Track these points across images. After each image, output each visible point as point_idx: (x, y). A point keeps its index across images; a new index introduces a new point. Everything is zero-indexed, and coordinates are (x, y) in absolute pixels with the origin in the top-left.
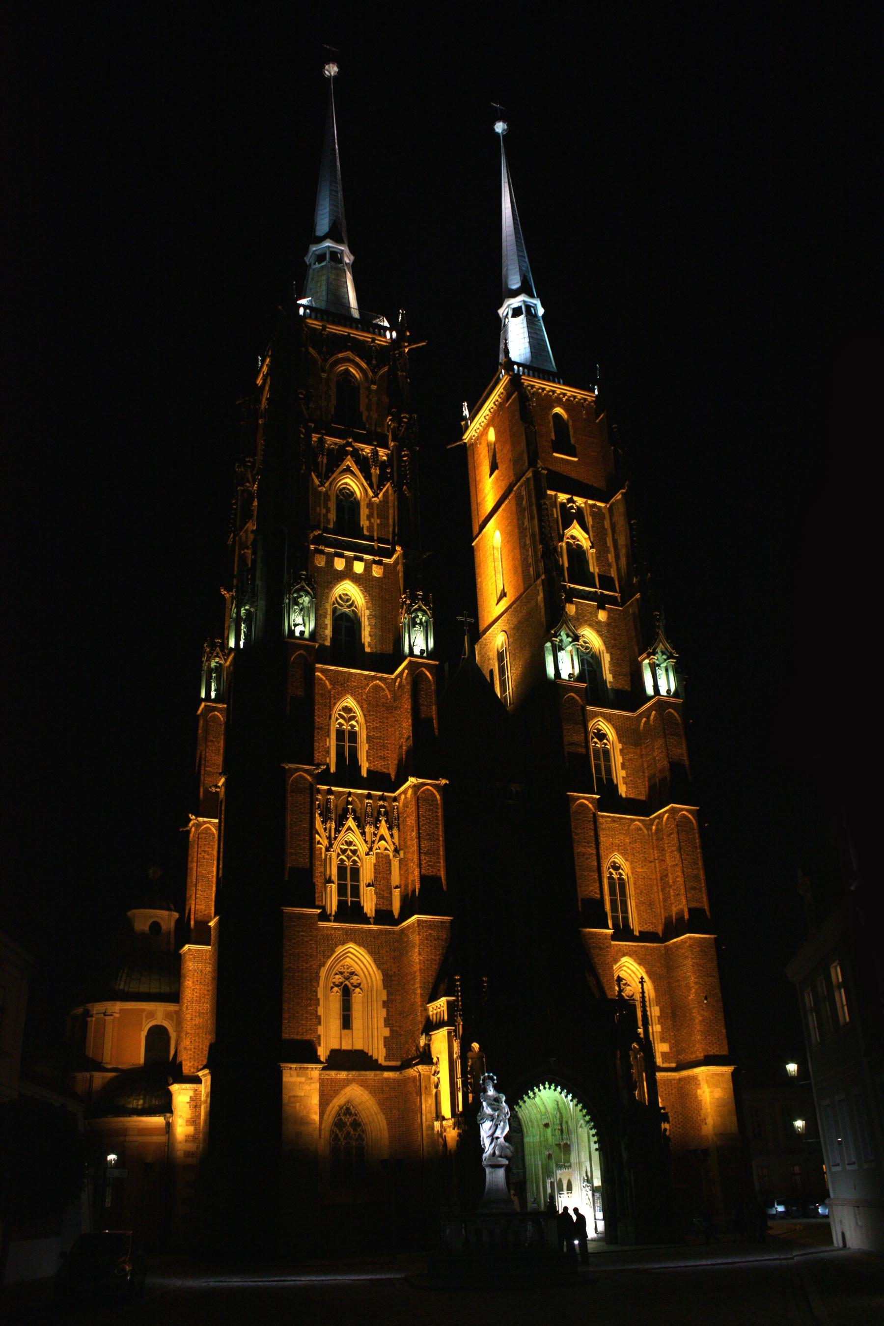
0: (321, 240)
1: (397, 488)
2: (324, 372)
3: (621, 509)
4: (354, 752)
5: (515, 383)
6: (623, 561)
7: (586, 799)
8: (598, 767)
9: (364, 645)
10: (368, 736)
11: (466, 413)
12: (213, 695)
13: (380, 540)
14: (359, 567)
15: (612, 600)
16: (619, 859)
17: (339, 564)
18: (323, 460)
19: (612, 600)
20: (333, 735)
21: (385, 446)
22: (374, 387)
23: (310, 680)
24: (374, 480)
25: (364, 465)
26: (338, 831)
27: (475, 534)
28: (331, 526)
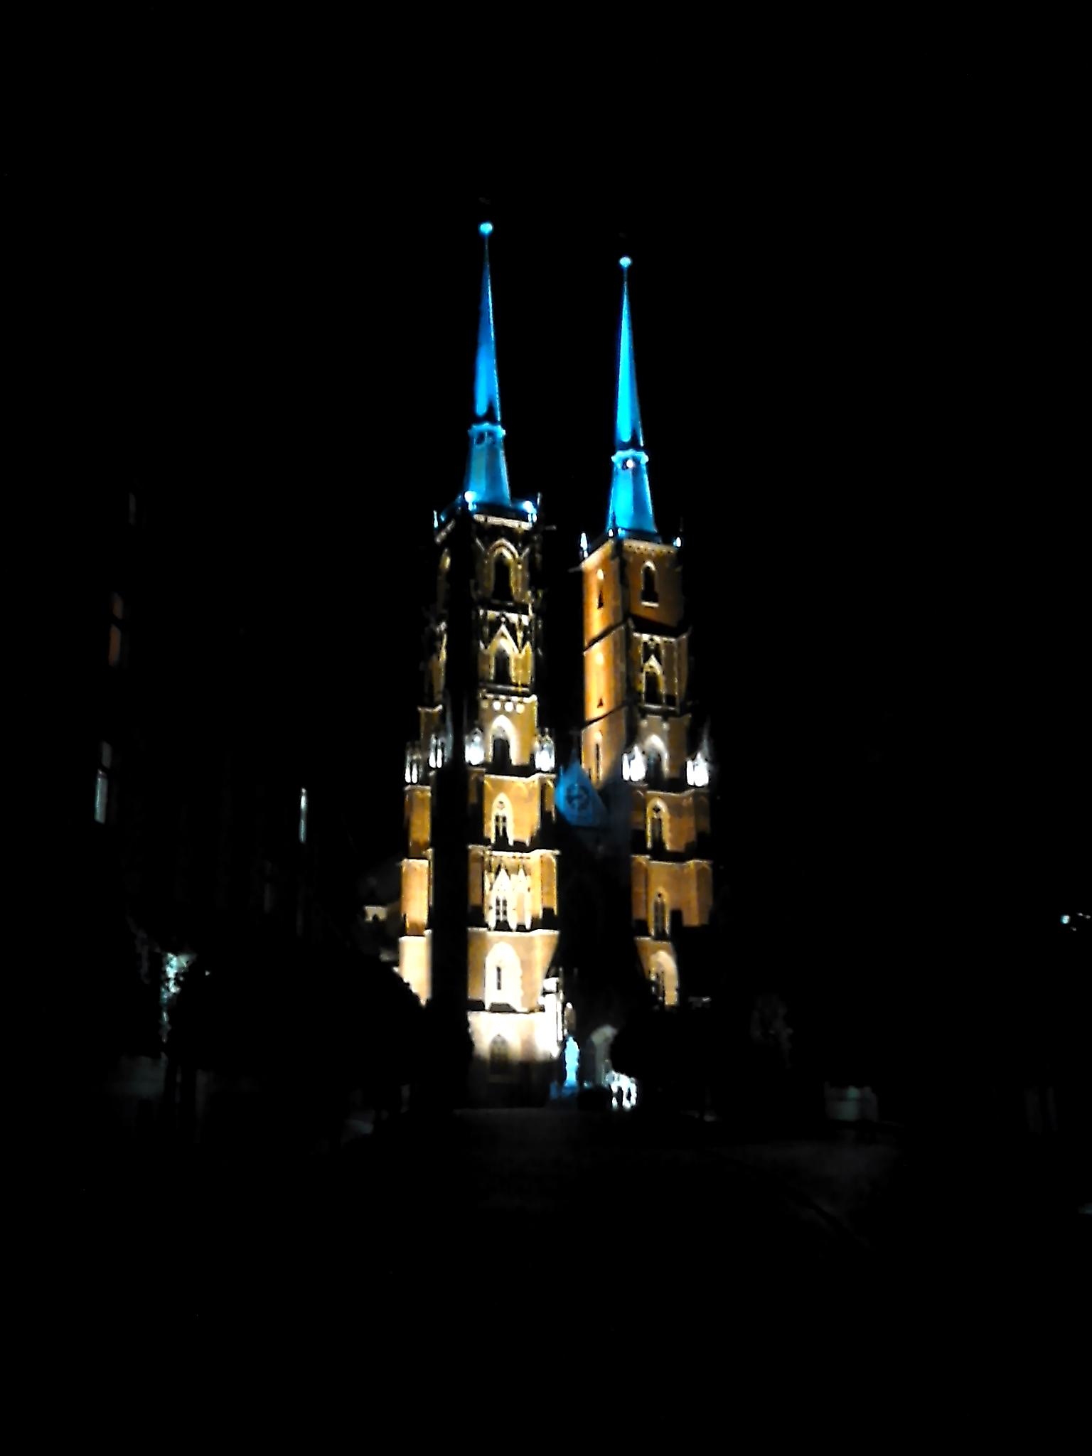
0: (479, 420)
1: (534, 649)
2: (486, 557)
3: (685, 647)
4: (504, 830)
5: (619, 546)
6: (684, 686)
7: (643, 859)
8: (653, 831)
9: (511, 761)
10: (515, 821)
11: (584, 543)
12: (415, 781)
13: (524, 686)
14: (509, 707)
15: (673, 714)
16: (661, 890)
17: (497, 705)
18: (487, 630)
19: (673, 714)
20: (493, 818)
21: (527, 614)
22: (520, 567)
23: (481, 786)
24: (520, 641)
25: (512, 629)
26: (496, 878)
27: (586, 644)
28: (492, 678)
